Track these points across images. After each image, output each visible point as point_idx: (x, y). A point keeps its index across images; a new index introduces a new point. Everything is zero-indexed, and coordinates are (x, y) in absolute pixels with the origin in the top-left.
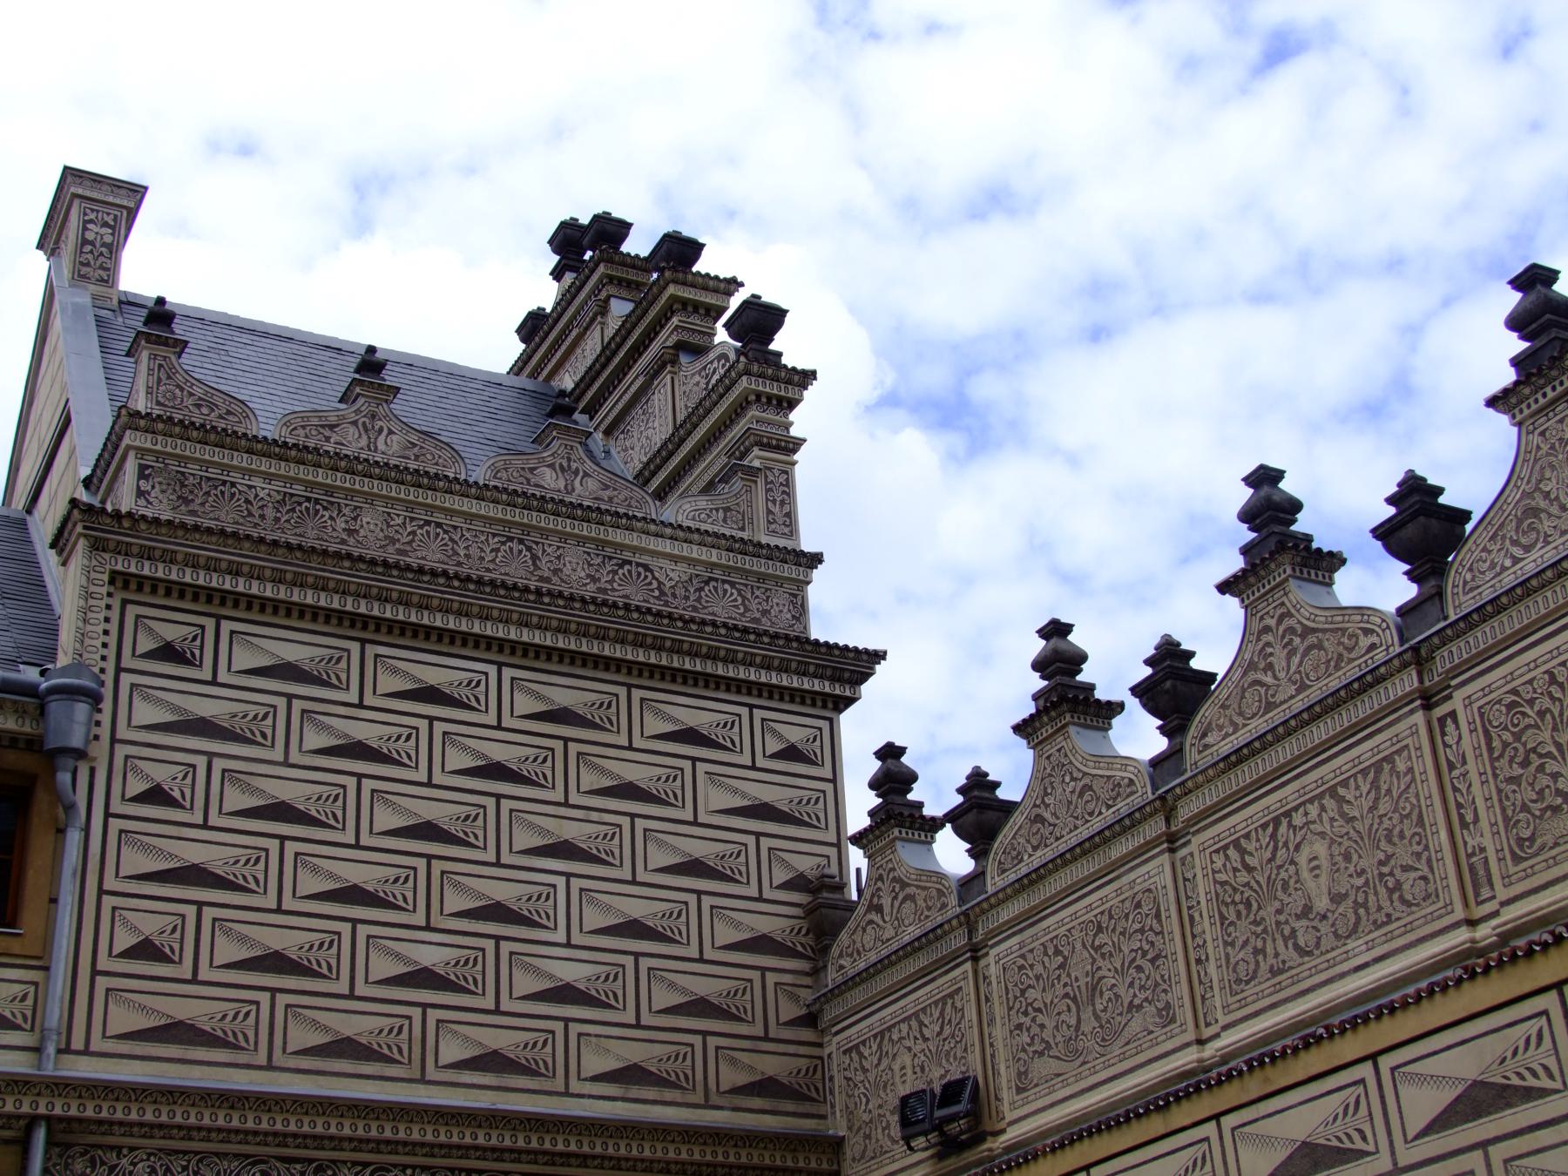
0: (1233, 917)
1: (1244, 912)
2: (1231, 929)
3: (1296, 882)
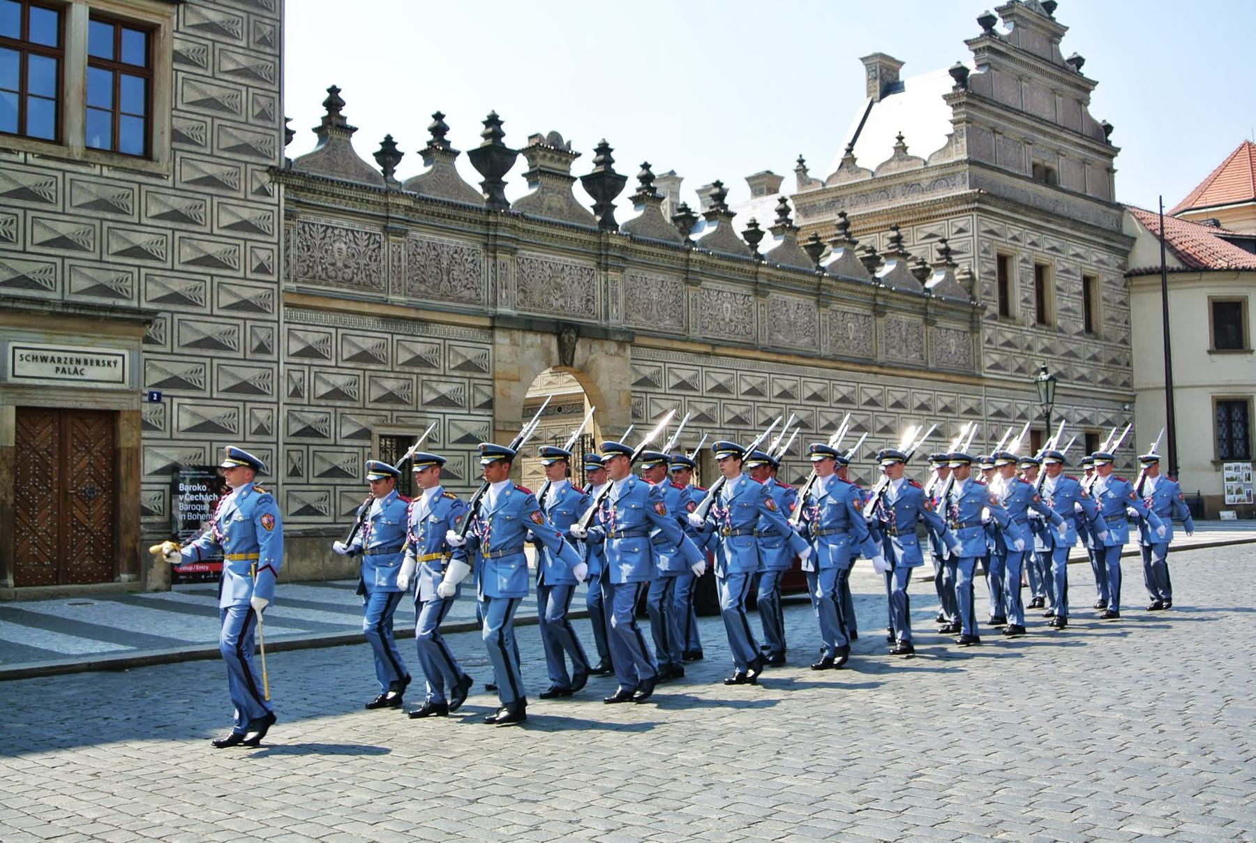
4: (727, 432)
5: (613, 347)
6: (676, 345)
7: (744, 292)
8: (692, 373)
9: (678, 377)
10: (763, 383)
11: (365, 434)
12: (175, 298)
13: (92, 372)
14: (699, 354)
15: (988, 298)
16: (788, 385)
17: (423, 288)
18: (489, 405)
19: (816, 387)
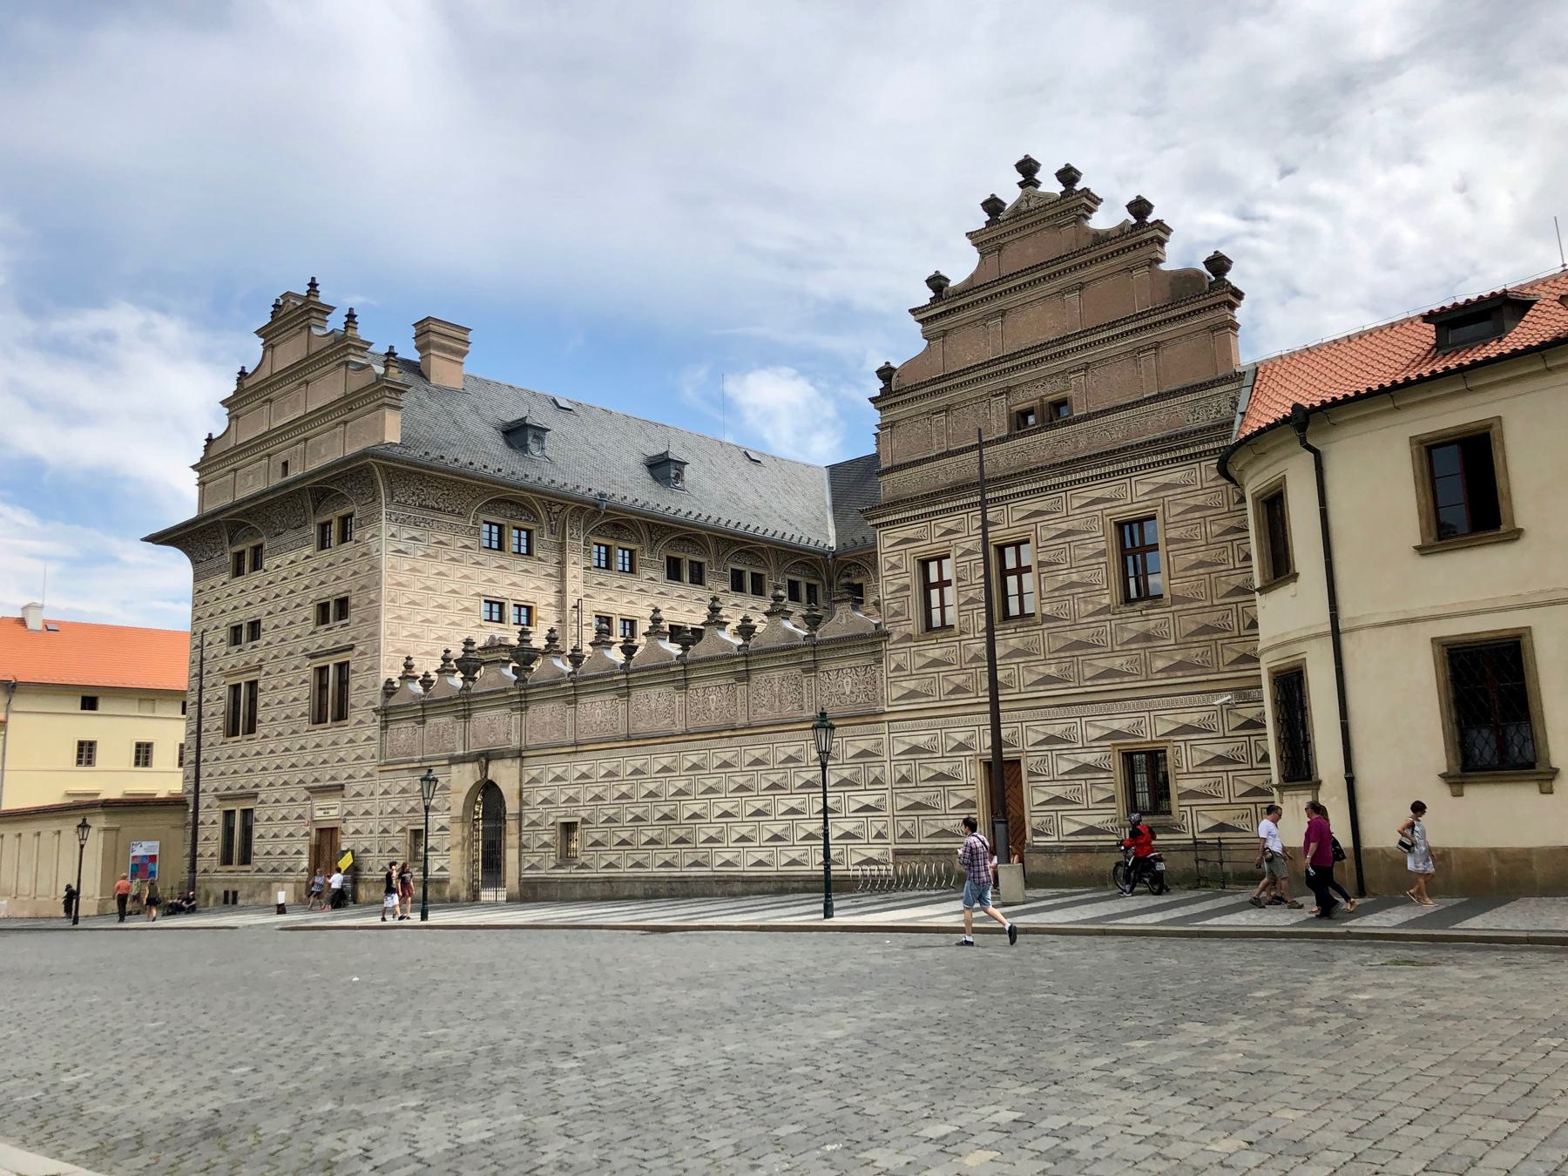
5: (508, 762)
6: (550, 751)
11: (403, 830)
12: (350, 777)
13: (332, 812)
15: (900, 618)
16: (638, 764)
17: (432, 748)
18: (449, 809)
19: (665, 761)
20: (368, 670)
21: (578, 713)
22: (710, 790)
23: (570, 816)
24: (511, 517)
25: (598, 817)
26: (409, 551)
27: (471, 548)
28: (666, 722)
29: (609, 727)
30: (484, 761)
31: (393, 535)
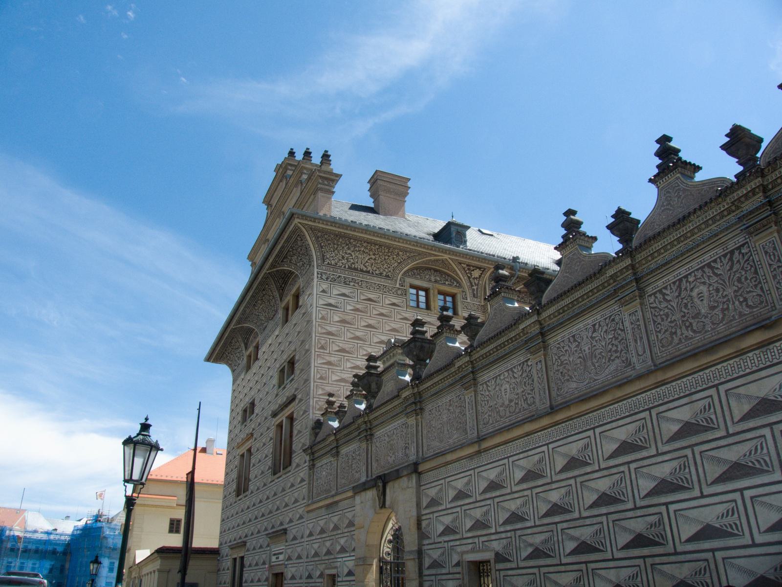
0: (659, 320)
1: (665, 319)
2: (659, 326)
3: (692, 303)
4: (503, 535)
7: (522, 359)
8: (466, 479)
9: (455, 488)
10: (540, 461)
11: (321, 575)
14: (470, 457)
16: (574, 449)
17: (343, 481)
19: (622, 434)
20: (303, 414)
21: (479, 397)
22: (736, 471)
23: (479, 551)
24: (436, 281)
25: (518, 549)
26: (339, 305)
27: (399, 306)
28: (613, 367)
29: (521, 403)
30: (381, 484)
31: (324, 291)
